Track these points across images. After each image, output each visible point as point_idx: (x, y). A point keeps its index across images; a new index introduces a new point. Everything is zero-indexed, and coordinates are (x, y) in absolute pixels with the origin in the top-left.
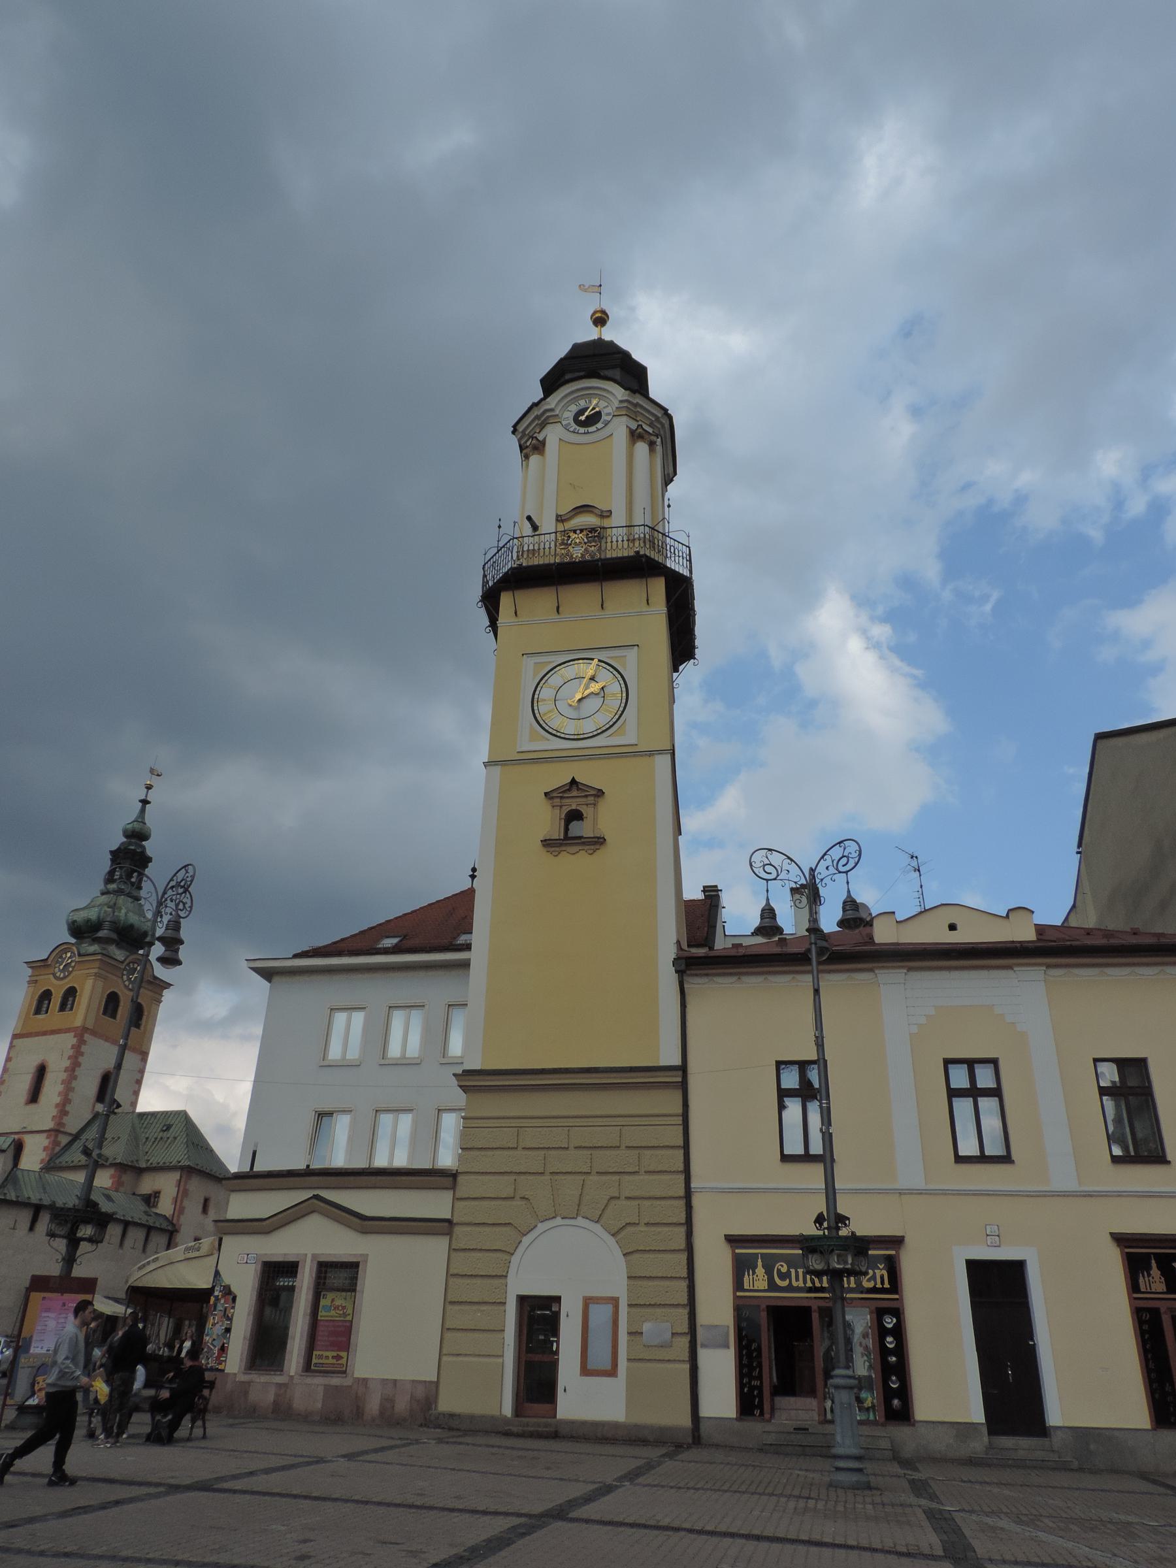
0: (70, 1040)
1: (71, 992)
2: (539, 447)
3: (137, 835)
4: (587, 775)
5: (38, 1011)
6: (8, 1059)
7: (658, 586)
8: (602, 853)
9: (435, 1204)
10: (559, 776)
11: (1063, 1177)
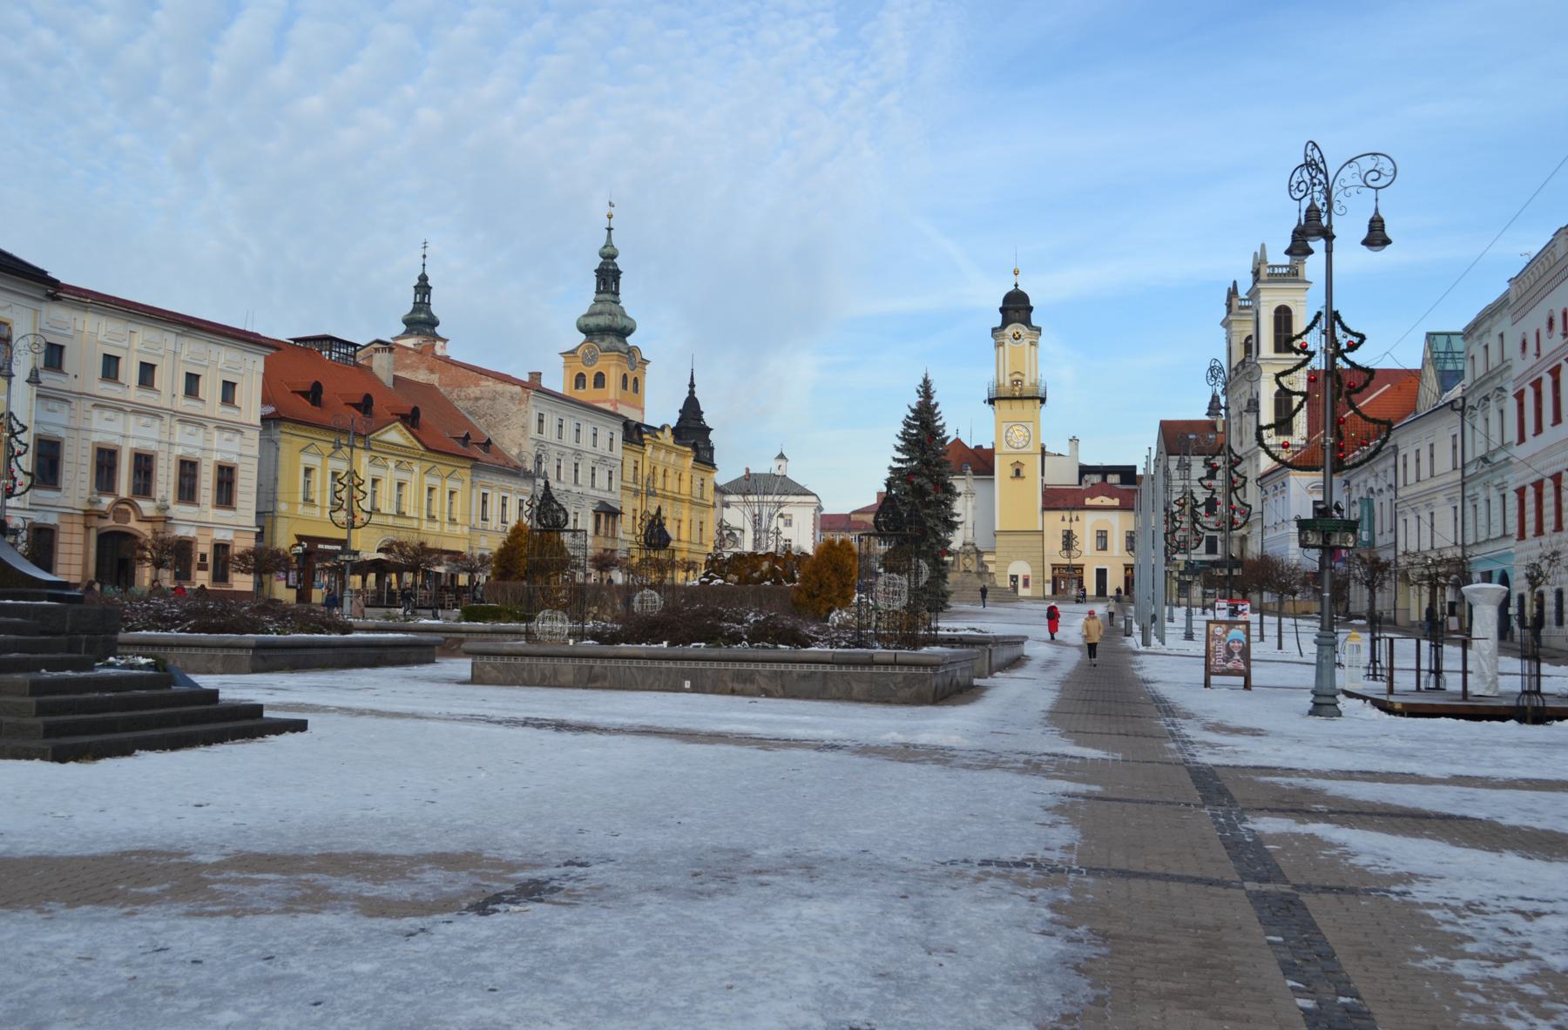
2: (1002, 344)
3: (609, 256)
5: (577, 387)
10: (1014, 459)
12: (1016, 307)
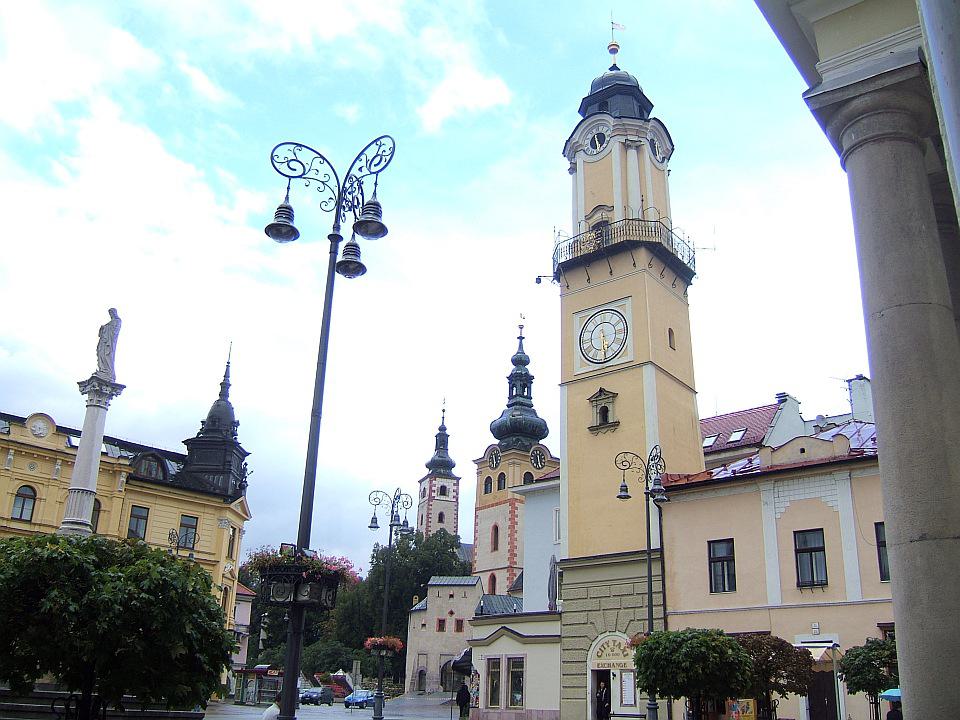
0: (507, 508)
1: (502, 477)
4: (609, 384)
6: (476, 524)
7: (642, 256)
8: (619, 429)
9: (553, 628)
10: (593, 388)
11: (854, 595)
12: (617, 101)
